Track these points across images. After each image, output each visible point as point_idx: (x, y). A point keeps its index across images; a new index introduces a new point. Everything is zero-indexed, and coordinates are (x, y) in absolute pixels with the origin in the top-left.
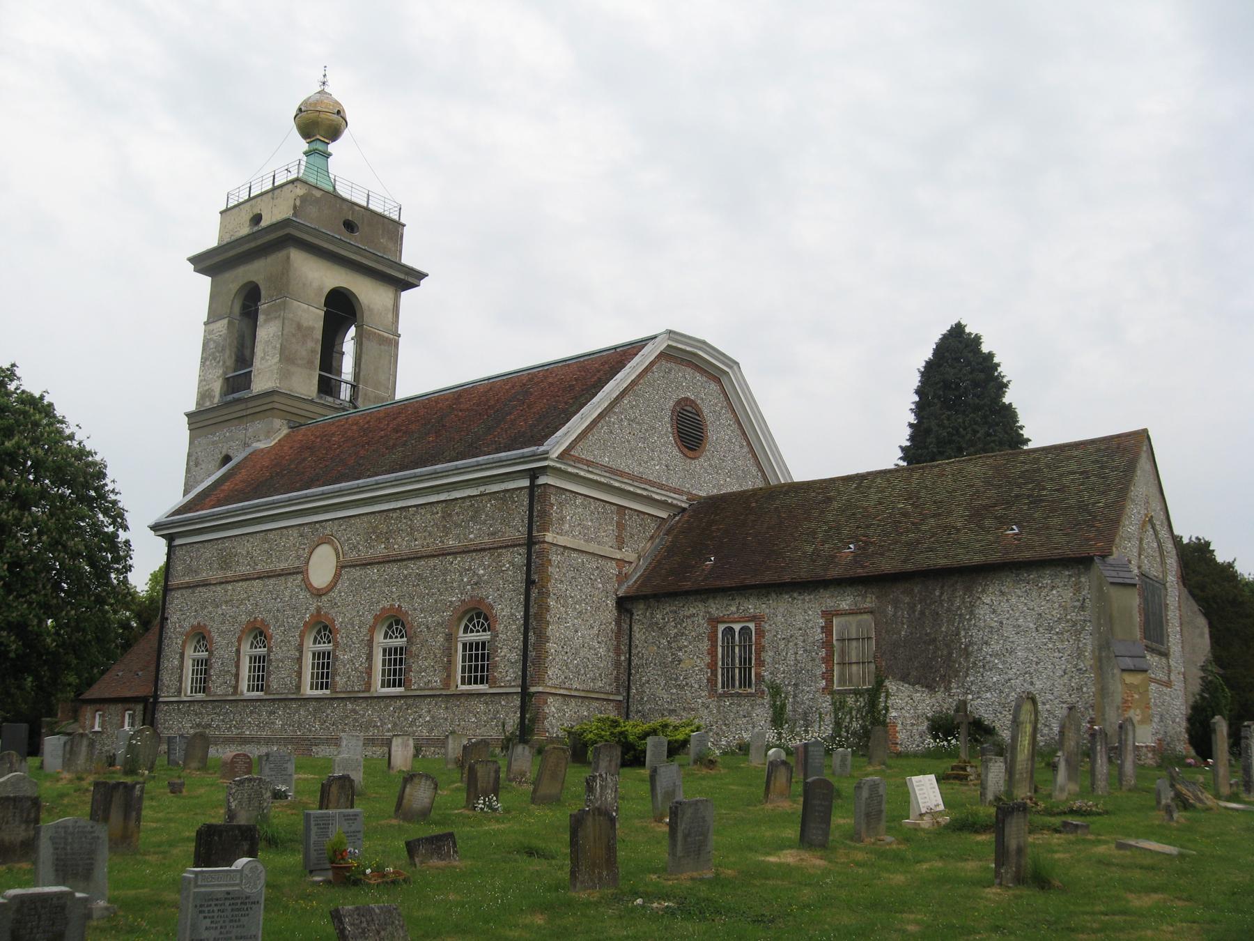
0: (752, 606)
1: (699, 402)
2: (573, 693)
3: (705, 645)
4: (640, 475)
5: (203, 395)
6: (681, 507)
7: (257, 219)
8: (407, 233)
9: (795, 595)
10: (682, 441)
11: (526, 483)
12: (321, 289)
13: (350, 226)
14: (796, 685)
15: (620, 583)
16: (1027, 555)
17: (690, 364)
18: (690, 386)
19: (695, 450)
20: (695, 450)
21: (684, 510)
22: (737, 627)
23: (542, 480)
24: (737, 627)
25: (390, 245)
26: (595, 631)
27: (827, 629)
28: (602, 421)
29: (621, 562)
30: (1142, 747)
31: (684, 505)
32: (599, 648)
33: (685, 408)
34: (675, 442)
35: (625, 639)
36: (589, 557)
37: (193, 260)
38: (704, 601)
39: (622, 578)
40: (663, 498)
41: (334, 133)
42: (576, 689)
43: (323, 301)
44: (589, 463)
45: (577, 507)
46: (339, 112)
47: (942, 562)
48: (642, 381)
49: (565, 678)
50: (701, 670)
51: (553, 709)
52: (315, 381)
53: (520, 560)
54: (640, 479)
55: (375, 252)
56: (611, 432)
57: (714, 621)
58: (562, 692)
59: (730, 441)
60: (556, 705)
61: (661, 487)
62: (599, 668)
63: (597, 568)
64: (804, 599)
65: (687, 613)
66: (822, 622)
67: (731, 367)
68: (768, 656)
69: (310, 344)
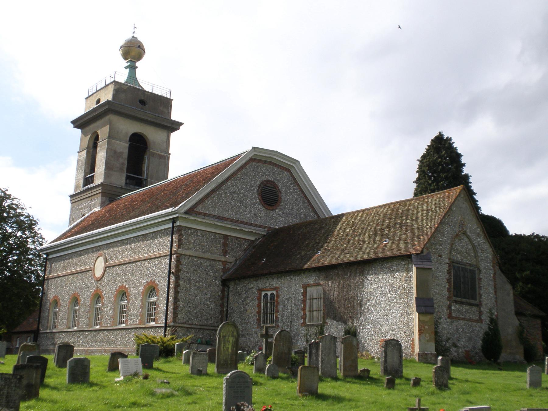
0: (275, 283)
2: (193, 326)
3: (256, 302)
4: (237, 219)
5: (77, 187)
6: (261, 234)
7: (98, 101)
8: (174, 104)
9: (292, 277)
10: (264, 201)
11: (170, 225)
14: (291, 322)
15: (224, 273)
16: (386, 254)
19: (273, 206)
20: (273, 206)
21: (264, 236)
22: (269, 293)
23: (178, 223)
24: (269, 293)
26: (208, 296)
27: (304, 294)
28: (214, 194)
29: (224, 263)
30: (429, 354)
31: (263, 233)
32: (211, 304)
33: (267, 185)
34: (260, 202)
35: (226, 300)
37: (73, 122)
38: (256, 281)
39: (224, 270)
40: (250, 230)
41: (139, 57)
42: (195, 325)
43: (128, 139)
44: (205, 215)
45: (198, 236)
47: (350, 259)
48: (239, 173)
49: (189, 319)
50: (254, 315)
51: (181, 334)
52: (124, 178)
53: (168, 262)
55: (154, 114)
56: (220, 199)
57: (260, 290)
58: (186, 325)
59: (296, 200)
60: (183, 332)
61: (251, 225)
62: (210, 314)
63: (210, 265)
64: (295, 279)
65: (250, 287)
66: (302, 290)
67: (295, 163)
68: (280, 308)
69: (121, 161)
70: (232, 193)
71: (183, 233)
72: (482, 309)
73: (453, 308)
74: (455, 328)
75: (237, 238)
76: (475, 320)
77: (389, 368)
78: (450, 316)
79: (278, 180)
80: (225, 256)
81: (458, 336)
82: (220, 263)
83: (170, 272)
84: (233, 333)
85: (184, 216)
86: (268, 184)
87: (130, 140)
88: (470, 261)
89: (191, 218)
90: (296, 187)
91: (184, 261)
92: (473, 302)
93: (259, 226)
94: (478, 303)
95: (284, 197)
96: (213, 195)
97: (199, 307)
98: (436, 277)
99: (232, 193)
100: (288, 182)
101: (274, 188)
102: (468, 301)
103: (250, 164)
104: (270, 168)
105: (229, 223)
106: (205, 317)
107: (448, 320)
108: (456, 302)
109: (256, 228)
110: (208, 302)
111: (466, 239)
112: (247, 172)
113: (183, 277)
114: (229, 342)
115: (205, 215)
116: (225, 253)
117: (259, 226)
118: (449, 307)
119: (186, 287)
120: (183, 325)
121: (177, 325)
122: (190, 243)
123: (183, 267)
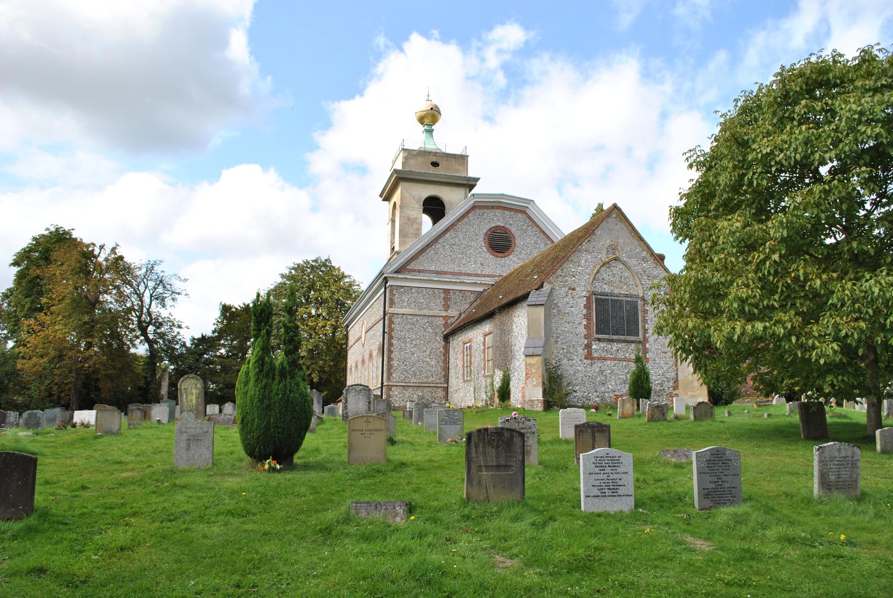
1: (507, 226)
2: (409, 384)
12: (420, 198)
13: (435, 164)
17: (498, 208)
18: (497, 220)
25: (461, 168)
26: (428, 353)
29: (446, 318)
36: (422, 318)
39: (446, 325)
44: (420, 271)
46: (432, 109)
54: (461, 274)
58: (401, 384)
59: (536, 243)
61: (477, 275)
67: (529, 204)
70: (451, 245)
71: (394, 292)
72: (647, 346)
73: (594, 347)
74: (597, 370)
75: (461, 291)
77: (350, 414)
78: (589, 356)
79: (511, 225)
80: (446, 311)
81: (603, 378)
82: (441, 319)
83: (384, 332)
84: (196, 385)
85: (392, 275)
87: (424, 205)
88: (626, 291)
89: (400, 276)
90: (535, 229)
91: (396, 320)
92: (633, 338)
93: (488, 276)
94: (642, 339)
95: (519, 242)
96: (428, 251)
97: (417, 365)
98: (565, 313)
99: (451, 245)
100: (523, 225)
102: (622, 337)
103: (473, 212)
104: (498, 212)
105: (449, 276)
106: (425, 375)
107: (585, 361)
108: (599, 340)
109: (483, 279)
110: (428, 359)
111: (621, 266)
112: (470, 221)
113: (397, 336)
114: (193, 394)
115: (420, 271)
116: (447, 307)
117: (488, 276)
118: (588, 346)
119: (401, 346)
120: (398, 384)
121: (391, 384)
122: (403, 301)
123: (396, 327)
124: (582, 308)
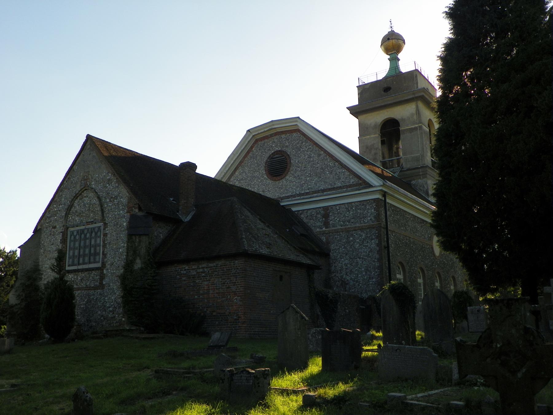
18: (274, 146)
33: (274, 157)
34: (268, 177)
48: (246, 159)
59: (310, 157)
67: (297, 121)
72: (105, 272)
76: (93, 287)
86: (274, 155)
101: (282, 156)
104: (275, 139)
124: (59, 244)
